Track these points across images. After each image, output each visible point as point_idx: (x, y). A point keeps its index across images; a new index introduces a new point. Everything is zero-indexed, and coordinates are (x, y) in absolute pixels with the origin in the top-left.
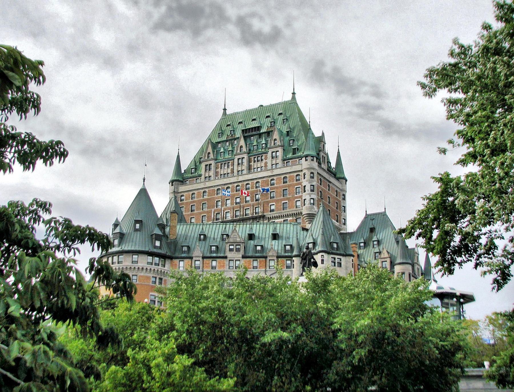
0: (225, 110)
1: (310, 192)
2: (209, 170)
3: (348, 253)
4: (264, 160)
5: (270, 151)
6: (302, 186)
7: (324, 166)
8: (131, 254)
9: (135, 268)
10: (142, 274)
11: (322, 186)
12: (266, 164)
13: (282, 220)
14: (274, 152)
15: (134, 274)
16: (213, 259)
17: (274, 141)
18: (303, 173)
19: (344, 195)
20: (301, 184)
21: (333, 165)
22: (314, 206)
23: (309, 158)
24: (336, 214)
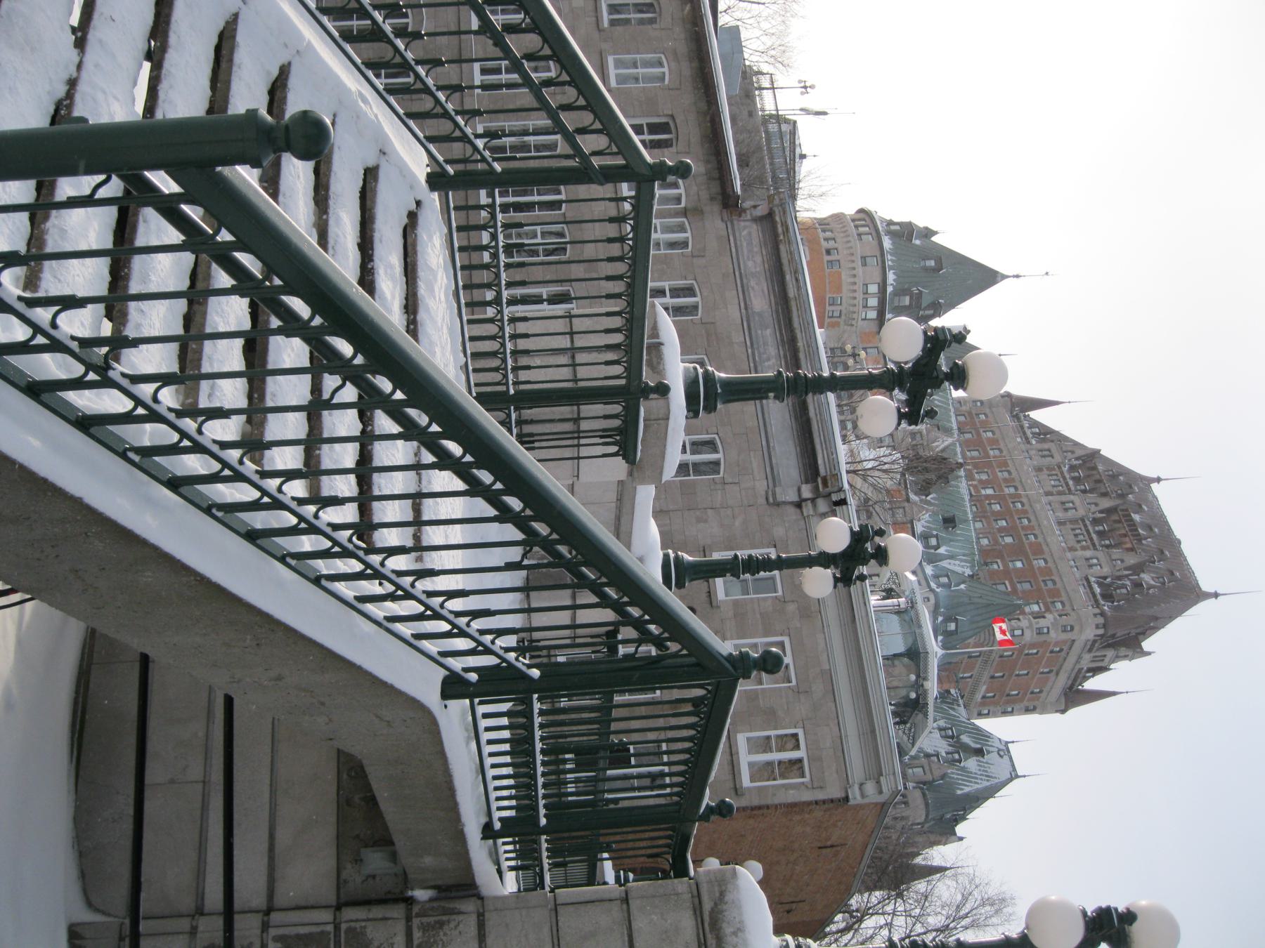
0: (1158, 480)
1: (1035, 626)
4: (1078, 546)
5: (1100, 554)
6: (1045, 612)
8: (878, 254)
11: (1048, 654)
20: (1048, 610)
23: (1101, 620)
24: (998, 694)
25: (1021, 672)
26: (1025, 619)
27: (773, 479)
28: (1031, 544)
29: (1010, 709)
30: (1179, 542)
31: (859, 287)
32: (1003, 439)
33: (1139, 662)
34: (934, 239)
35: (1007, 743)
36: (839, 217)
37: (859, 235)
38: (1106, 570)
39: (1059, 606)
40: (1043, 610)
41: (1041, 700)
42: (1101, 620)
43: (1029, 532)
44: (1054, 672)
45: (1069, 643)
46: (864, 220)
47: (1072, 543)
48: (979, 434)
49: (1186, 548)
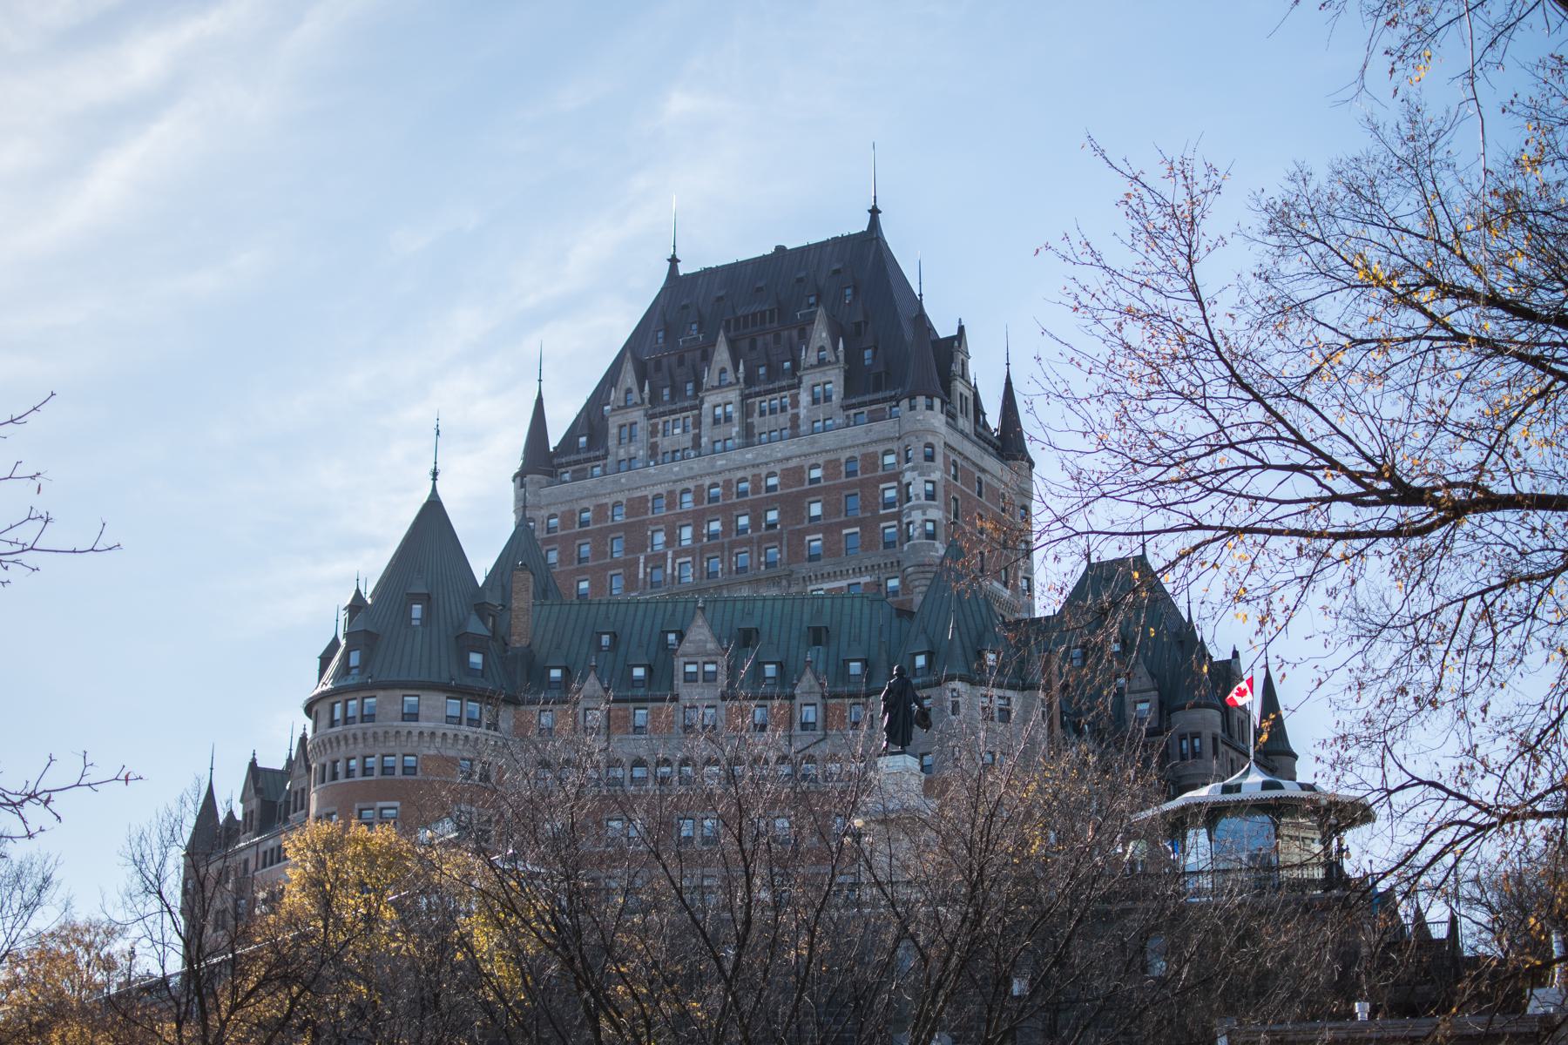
0: (674, 261)
1: (923, 500)
2: (630, 441)
4: (790, 411)
6: (900, 482)
7: (967, 424)
8: (399, 693)
9: (410, 733)
10: (432, 752)
12: (796, 417)
13: (844, 583)
16: (637, 705)
20: (896, 476)
21: (993, 420)
22: (937, 544)
28: (783, 484)
30: (780, 249)
31: (450, 729)
32: (596, 496)
38: (834, 380)
39: (890, 459)
40: (895, 484)
42: (921, 401)
47: (783, 420)
48: (585, 534)
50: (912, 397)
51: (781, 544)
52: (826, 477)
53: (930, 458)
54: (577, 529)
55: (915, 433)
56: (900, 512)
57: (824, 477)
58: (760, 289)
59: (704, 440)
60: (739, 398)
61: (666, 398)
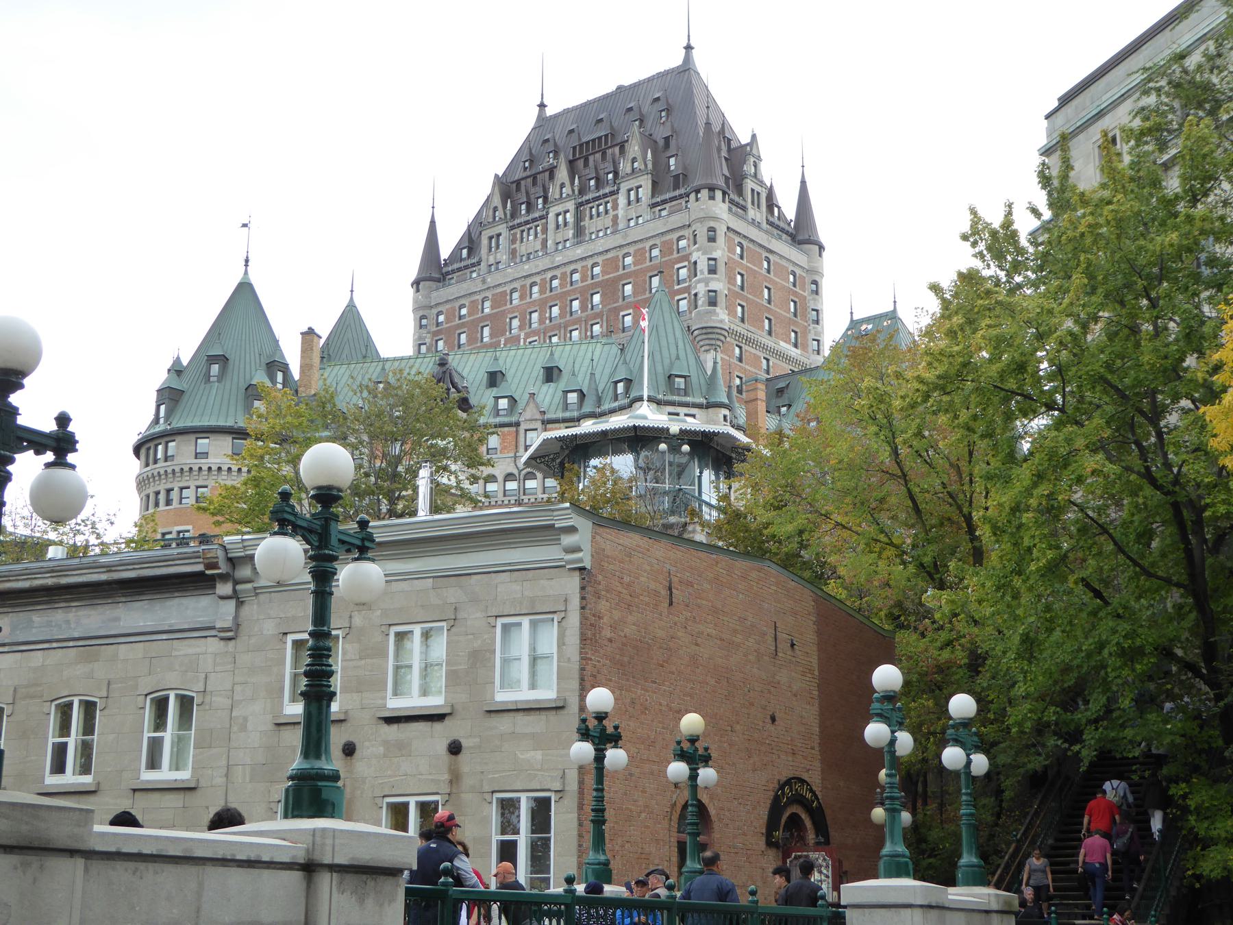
0: (542, 106)
3: (712, 400)
4: (611, 213)
5: (624, 187)
6: (689, 262)
7: (758, 215)
8: (193, 437)
9: (200, 469)
11: (744, 262)
14: (632, 189)
15: (199, 483)
17: (633, 163)
18: (691, 231)
19: (815, 283)
20: (686, 258)
22: (718, 309)
23: (704, 194)
24: (792, 327)
25: (766, 296)
26: (696, 287)
27: (203, 630)
28: (604, 272)
29: (815, 313)
33: (764, 148)
34: (185, 362)
35: (852, 320)
36: (142, 483)
37: (166, 459)
38: (646, 182)
39: (683, 243)
40: (686, 263)
41: (804, 275)
42: (704, 194)
43: (589, 273)
44: (767, 255)
45: (731, 235)
46: (149, 449)
48: (463, 325)
49: (628, 81)
50: (698, 191)
51: (602, 320)
52: (635, 264)
53: (712, 240)
54: (457, 321)
55: (701, 220)
56: (690, 286)
57: (634, 263)
58: (601, 120)
59: (549, 242)
60: (573, 207)
61: (523, 212)
